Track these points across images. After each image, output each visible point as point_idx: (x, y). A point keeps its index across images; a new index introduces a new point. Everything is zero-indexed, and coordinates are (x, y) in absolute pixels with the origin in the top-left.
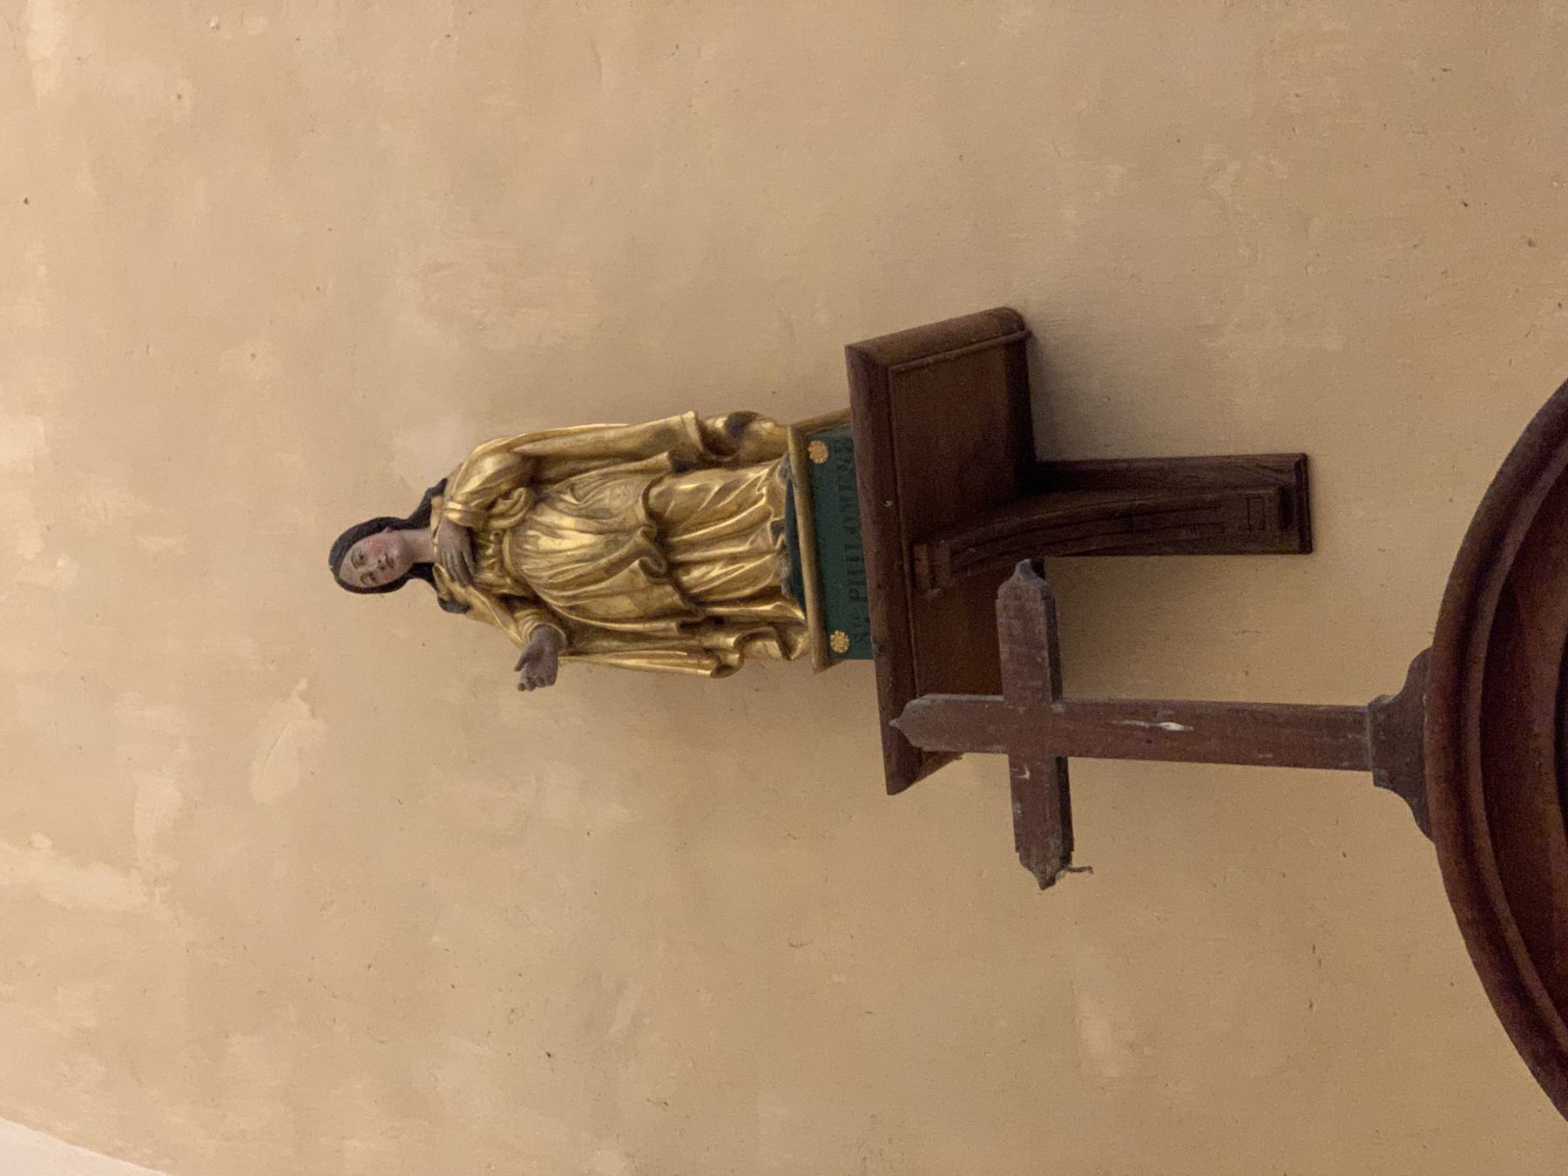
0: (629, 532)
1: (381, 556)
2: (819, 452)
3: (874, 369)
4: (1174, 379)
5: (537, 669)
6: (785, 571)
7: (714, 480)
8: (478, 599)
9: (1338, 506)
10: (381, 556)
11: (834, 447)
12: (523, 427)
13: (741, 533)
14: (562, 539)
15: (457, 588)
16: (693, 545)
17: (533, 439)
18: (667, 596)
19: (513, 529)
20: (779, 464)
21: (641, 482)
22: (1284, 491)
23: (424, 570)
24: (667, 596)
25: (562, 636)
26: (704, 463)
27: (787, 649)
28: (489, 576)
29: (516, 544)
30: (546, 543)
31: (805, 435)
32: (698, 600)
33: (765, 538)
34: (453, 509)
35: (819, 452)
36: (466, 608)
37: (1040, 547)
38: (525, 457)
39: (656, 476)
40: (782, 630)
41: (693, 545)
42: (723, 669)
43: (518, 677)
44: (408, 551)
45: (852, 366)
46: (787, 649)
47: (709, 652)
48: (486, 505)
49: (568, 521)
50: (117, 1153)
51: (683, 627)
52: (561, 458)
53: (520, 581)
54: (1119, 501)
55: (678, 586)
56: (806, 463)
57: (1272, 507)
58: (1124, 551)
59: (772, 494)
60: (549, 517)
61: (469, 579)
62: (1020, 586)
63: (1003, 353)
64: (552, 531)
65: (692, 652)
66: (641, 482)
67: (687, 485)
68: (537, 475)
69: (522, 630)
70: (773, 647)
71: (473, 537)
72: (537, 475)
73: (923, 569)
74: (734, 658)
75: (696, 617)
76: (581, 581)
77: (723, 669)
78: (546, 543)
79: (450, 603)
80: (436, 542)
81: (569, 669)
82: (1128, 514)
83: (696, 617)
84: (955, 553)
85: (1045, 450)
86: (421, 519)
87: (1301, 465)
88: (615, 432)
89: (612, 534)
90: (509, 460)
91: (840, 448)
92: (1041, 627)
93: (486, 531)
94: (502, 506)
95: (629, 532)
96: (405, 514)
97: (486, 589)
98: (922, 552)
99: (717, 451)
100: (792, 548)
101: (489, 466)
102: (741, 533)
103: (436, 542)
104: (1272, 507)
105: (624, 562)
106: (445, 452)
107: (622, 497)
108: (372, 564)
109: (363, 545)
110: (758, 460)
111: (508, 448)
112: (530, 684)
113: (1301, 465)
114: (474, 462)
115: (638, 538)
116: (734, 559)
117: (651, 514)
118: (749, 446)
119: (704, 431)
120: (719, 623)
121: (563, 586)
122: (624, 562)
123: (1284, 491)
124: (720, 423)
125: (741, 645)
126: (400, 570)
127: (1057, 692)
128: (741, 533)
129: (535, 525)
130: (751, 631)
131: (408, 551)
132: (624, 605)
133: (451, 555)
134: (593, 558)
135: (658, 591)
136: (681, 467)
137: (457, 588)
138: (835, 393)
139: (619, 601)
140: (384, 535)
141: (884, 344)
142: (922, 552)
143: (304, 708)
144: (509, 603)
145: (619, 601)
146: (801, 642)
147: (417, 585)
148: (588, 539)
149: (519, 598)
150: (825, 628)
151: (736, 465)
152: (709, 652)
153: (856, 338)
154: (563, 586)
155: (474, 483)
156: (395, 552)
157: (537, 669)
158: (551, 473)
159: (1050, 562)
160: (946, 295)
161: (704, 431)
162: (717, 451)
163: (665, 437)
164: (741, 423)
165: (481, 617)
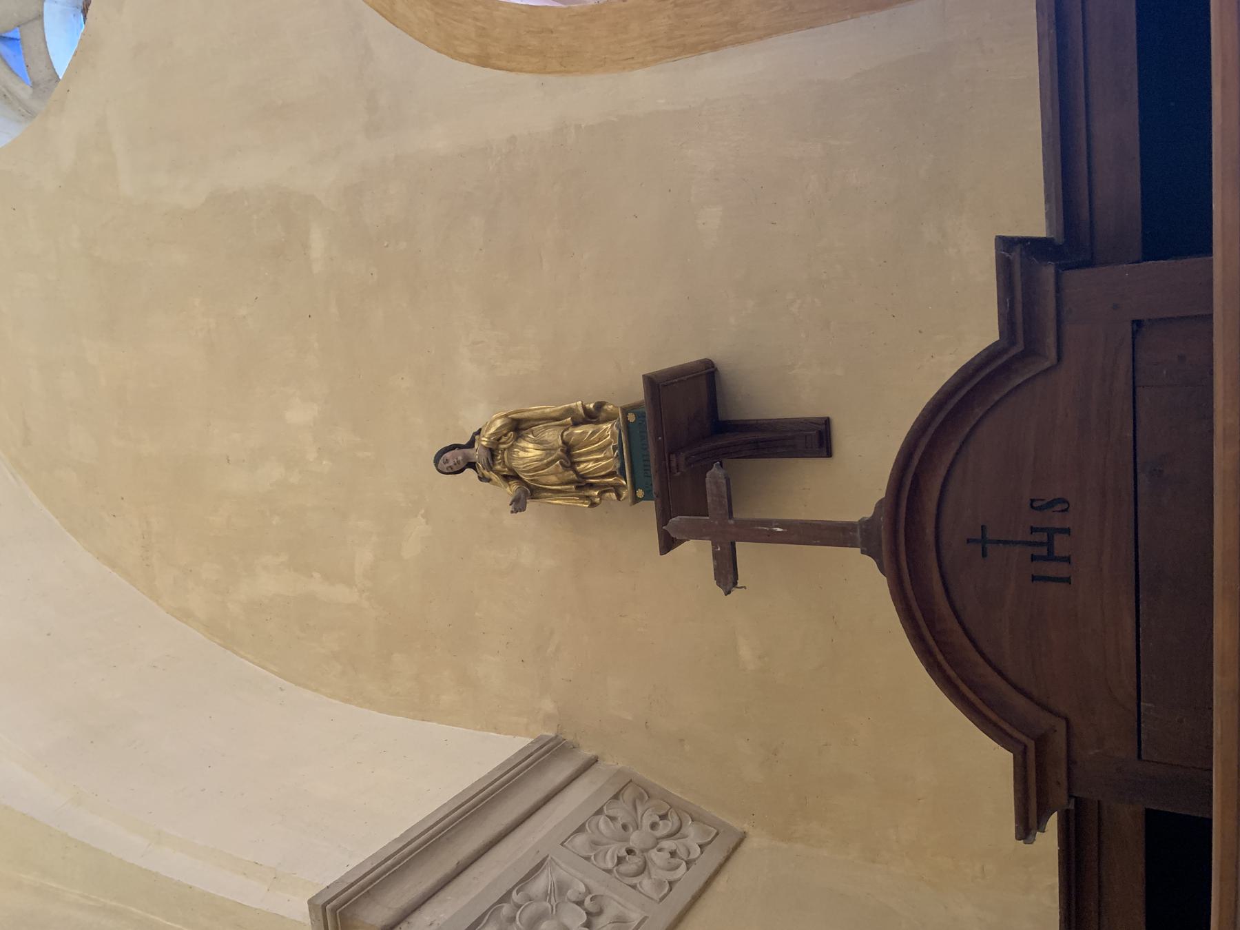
0: (556, 449)
1: (454, 459)
2: (632, 418)
3: (654, 384)
4: (779, 384)
5: (518, 505)
6: (618, 465)
7: (589, 429)
8: (494, 477)
9: (842, 438)
10: (454, 459)
11: (638, 416)
12: (513, 407)
13: (601, 450)
14: (528, 452)
15: (486, 472)
16: (581, 455)
17: (516, 412)
18: (571, 475)
19: (509, 448)
20: (616, 422)
21: (560, 430)
22: (820, 433)
23: (472, 465)
24: (571, 475)
25: (528, 492)
26: (585, 422)
27: (619, 496)
28: (498, 467)
29: (510, 454)
30: (522, 454)
31: (625, 411)
32: (584, 477)
33: (610, 452)
34: (484, 441)
35: (632, 418)
36: (489, 480)
37: (719, 455)
38: (514, 420)
39: (566, 427)
40: (617, 489)
41: (581, 455)
42: (593, 505)
43: (511, 508)
44: (466, 457)
45: (644, 383)
46: (619, 496)
47: (588, 497)
48: (497, 439)
49: (531, 445)
50: (347, 701)
51: (577, 487)
52: (527, 420)
53: (511, 469)
54: (751, 436)
55: (576, 472)
56: (626, 422)
57: (815, 439)
58: (756, 457)
59: (613, 434)
60: (523, 444)
61: (491, 469)
62: (715, 474)
63: (705, 376)
64: (524, 449)
65: (581, 498)
66: (560, 430)
67: (578, 431)
68: (518, 427)
69: (512, 489)
70: (613, 495)
71: (492, 452)
72: (518, 427)
73: (674, 464)
74: (598, 500)
75: (582, 484)
76: (536, 469)
77: (593, 505)
78: (522, 454)
79: (482, 478)
80: (477, 454)
81: (531, 505)
82: (756, 442)
83: (582, 484)
84: (686, 459)
85: (722, 416)
86: (471, 444)
87: (827, 422)
88: (549, 409)
89: (549, 450)
90: (507, 421)
91: (640, 416)
92: (724, 489)
93: (498, 449)
94: (503, 440)
95: (556, 449)
96: (464, 443)
97: (497, 473)
98: (673, 457)
99: (592, 416)
100: (620, 456)
101: (499, 423)
102: (601, 450)
103: (477, 454)
104: (815, 439)
105: (554, 461)
106: (480, 417)
107: (552, 436)
108: (451, 463)
109: (448, 455)
110: (605, 421)
111: (506, 416)
112: (515, 511)
113: (827, 422)
114: (492, 422)
115: (559, 452)
116: (597, 460)
117: (564, 442)
118: (603, 415)
119: (584, 408)
120: (591, 486)
121: (528, 471)
122: (554, 461)
123: (820, 433)
124: (591, 406)
125: (600, 495)
126: (462, 465)
127: (731, 513)
128: (600, 450)
129: (517, 447)
130: (604, 489)
131: (466, 457)
132: (553, 479)
133: (483, 459)
134: (541, 460)
135: (566, 473)
136: (576, 424)
137: (486, 472)
138: (638, 394)
139: (551, 478)
140: (456, 451)
141: (657, 374)
142: (673, 457)
143: (423, 521)
144: (506, 478)
145: (551, 478)
146: (624, 493)
147: (469, 471)
148: (538, 452)
149: (511, 476)
150: (635, 487)
151: (598, 423)
152: (588, 497)
153: (646, 372)
154: (528, 471)
155: (492, 430)
156: (460, 458)
157: (518, 505)
158: (523, 426)
159: (726, 461)
160: (682, 354)
161: (584, 408)
162: (592, 416)
163: (569, 412)
164: (600, 406)
165: (495, 484)
